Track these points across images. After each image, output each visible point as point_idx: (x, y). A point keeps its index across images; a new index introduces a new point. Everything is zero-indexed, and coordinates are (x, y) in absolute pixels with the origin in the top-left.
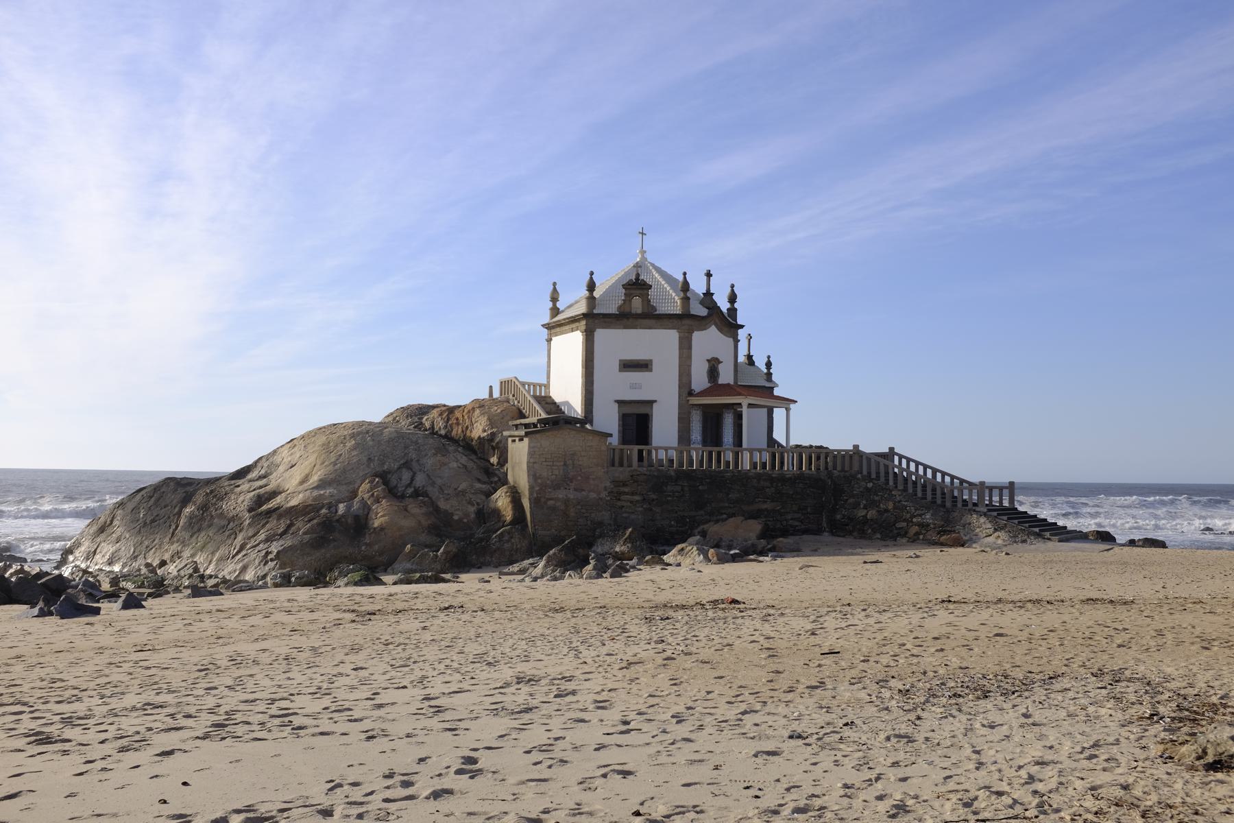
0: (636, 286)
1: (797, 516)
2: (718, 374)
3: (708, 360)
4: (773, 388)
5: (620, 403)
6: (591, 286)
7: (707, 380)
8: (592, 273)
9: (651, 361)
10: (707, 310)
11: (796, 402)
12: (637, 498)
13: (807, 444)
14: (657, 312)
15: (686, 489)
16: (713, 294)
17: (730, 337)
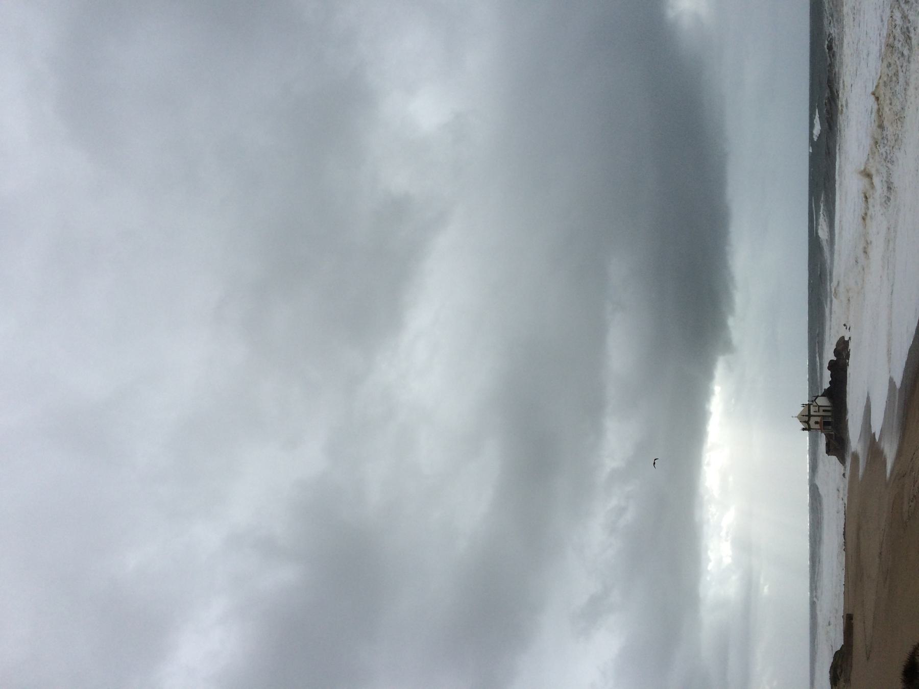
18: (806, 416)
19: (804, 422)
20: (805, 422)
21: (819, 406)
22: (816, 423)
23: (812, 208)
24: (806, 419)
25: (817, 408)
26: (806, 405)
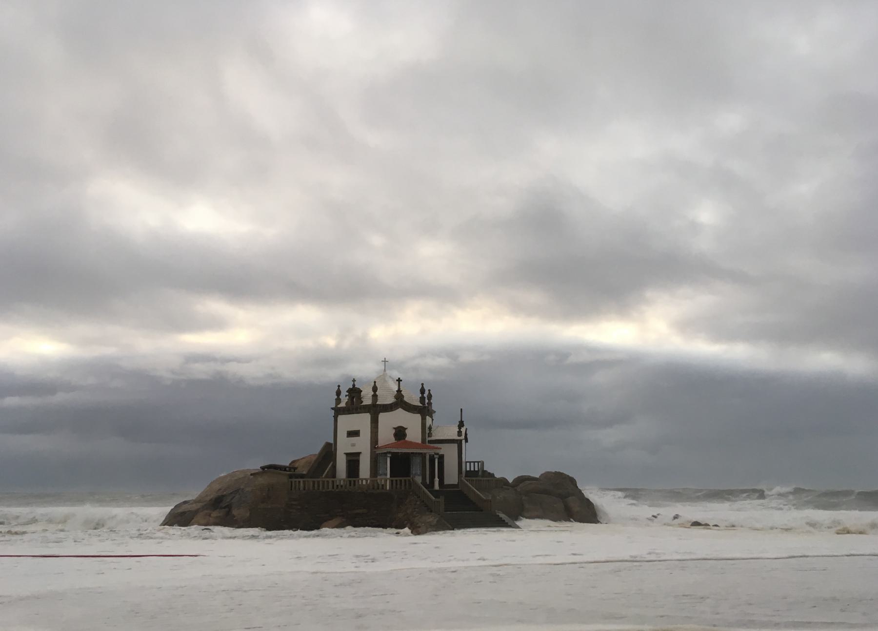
2: (405, 435)
3: (394, 428)
5: (347, 454)
6: (338, 393)
7: (394, 439)
8: (339, 386)
9: (359, 431)
10: (396, 400)
12: (299, 507)
13: (554, 471)
14: (363, 404)
16: (401, 391)
19: (399, 391)
20: (399, 394)
21: (459, 443)
22: (400, 433)
23: (534, 480)
24: (412, 397)
25: (456, 438)
26: (430, 404)
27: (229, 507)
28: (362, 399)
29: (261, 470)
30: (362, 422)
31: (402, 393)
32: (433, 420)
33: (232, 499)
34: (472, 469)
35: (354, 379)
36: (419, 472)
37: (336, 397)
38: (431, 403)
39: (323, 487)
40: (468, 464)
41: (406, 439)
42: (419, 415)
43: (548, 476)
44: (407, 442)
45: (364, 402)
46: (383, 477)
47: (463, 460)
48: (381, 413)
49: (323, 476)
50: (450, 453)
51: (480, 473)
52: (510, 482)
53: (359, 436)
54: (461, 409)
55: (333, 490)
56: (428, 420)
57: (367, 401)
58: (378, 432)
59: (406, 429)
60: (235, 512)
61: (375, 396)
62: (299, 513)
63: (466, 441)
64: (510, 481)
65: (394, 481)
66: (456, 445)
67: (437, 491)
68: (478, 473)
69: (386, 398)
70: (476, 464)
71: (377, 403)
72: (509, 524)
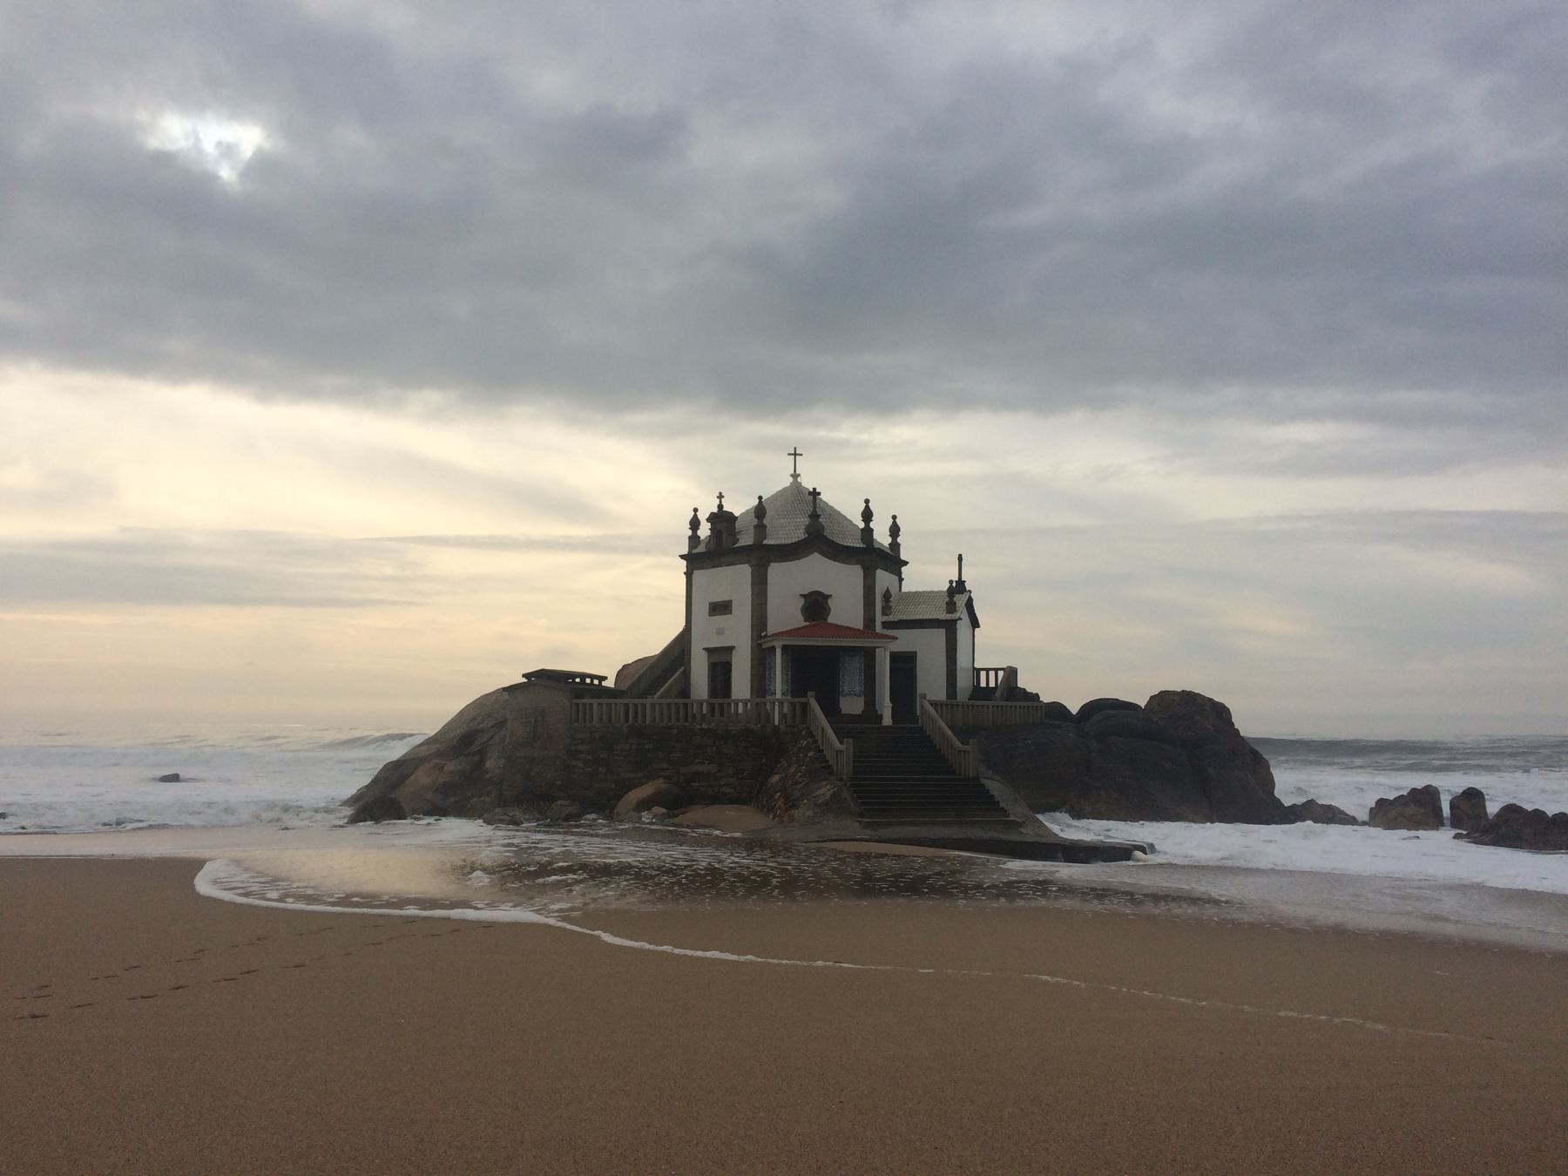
0: (721, 519)
1: (731, 780)
3: (801, 595)
4: (957, 620)
5: (709, 650)
8: (696, 510)
10: (806, 535)
11: (897, 638)
13: (1179, 690)
15: (633, 747)
17: (857, 564)
18: (867, 532)
19: (814, 516)
21: (950, 627)
22: (816, 605)
25: (944, 616)
26: (895, 546)
27: (482, 752)
28: (738, 537)
29: (524, 680)
30: (734, 581)
31: (820, 520)
32: (901, 580)
33: (491, 738)
34: (992, 684)
35: (720, 493)
36: (858, 689)
37: (690, 533)
38: (899, 545)
39: (636, 717)
40: (983, 674)
41: (831, 619)
42: (859, 566)
43: (1163, 700)
44: (830, 624)
45: (740, 541)
46: (773, 697)
47: (962, 661)
48: (772, 564)
49: (656, 696)
50: (928, 648)
51: (998, 694)
52: (1074, 713)
53: (731, 613)
54: (960, 556)
55: (686, 724)
56: (883, 578)
57: (746, 540)
58: (766, 604)
59: (831, 596)
60: (489, 764)
61: (761, 528)
62: (589, 769)
63: (975, 623)
64: (1074, 708)
65: (717, 706)
66: (940, 635)
67: (886, 727)
68: (994, 693)
69: (786, 531)
70: (992, 674)
71: (765, 542)
72: (1002, 805)
